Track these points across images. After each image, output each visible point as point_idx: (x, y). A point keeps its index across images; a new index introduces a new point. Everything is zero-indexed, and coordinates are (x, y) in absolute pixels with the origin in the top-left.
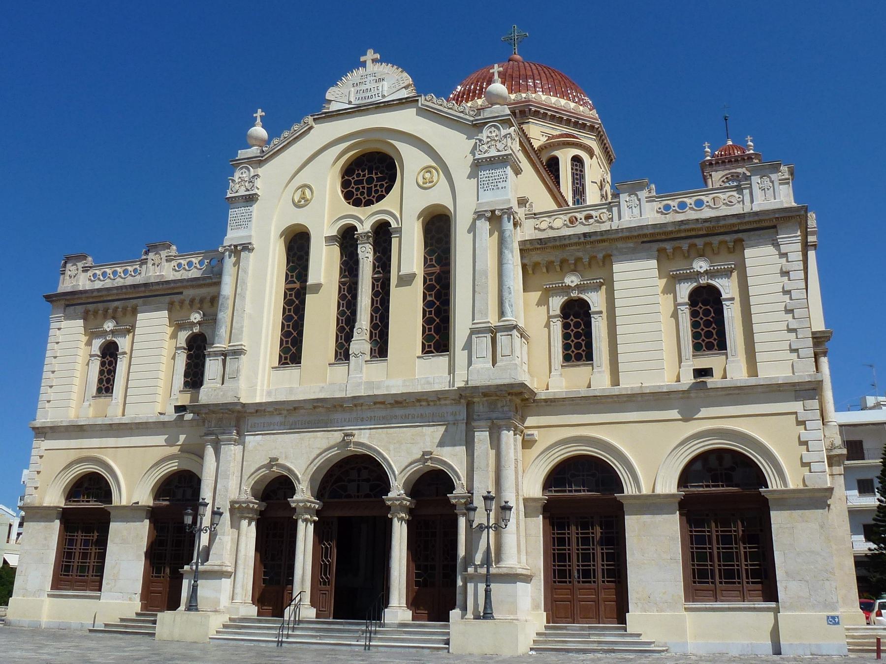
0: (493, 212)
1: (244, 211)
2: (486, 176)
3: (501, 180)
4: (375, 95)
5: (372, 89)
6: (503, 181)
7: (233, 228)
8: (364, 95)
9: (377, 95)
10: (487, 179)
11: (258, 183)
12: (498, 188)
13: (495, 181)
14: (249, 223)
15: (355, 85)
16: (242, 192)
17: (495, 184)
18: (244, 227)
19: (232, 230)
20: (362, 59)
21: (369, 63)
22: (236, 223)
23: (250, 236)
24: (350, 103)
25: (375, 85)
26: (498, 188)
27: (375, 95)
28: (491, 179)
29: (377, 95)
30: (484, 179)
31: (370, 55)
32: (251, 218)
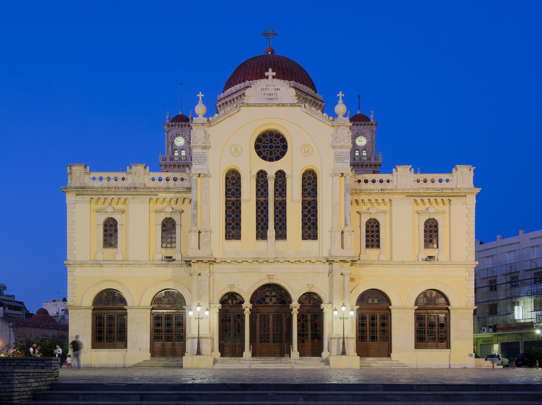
1: (201, 155)
2: (338, 155)
3: (346, 158)
4: (275, 98)
5: (273, 94)
6: (347, 159)
7: (196, 163)
10: (339, 156)
12: (344, 162)
13: (343, 158)
15: (263, 89)
17: (343, 160)
19: (195, 164)
20: (266, 74)
21: (270, 77)
22: (197, 161)
25: (275, 92)
26: (344, 162)
27: (275, 98)
28: (341, 157)
29: (276, 99)
30: (337, 156)
31: (270, 73)
32: (206, 159)
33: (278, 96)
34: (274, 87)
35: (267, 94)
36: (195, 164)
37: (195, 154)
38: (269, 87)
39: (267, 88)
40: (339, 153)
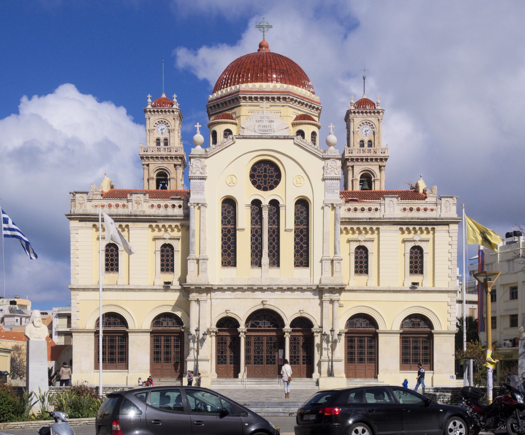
0: (332, 204)
1: (199, 185)
3: (336, 189)
5: (268, 126)
8: (263, 129)
9: (270, 130)
10: (329, 187)
11: (207, 170)
14: (203, 192)
15: (257, 121)
16: (198, 174)
18: (201, 194)
19: (193, 194)
23: (205, 200)
24: (255, 132)
25: (269, 124)
26: (334, 193)
28: (331, 187)
29: (270, 130)
30: (328, 187)
33: (272, 127)
34: (268, 119)
35: (262, 126)
36: (193, 194)
37: (193, 184)
38: (263, 119)
39: (261, 120)
40: (329, 184)
